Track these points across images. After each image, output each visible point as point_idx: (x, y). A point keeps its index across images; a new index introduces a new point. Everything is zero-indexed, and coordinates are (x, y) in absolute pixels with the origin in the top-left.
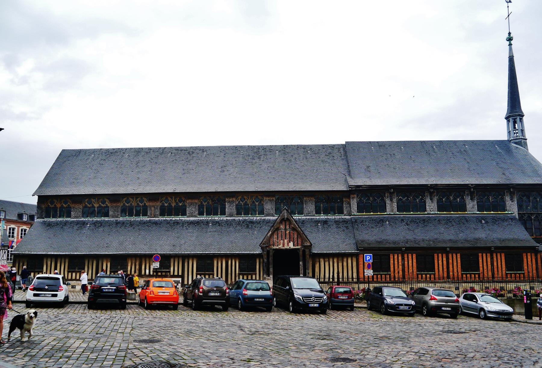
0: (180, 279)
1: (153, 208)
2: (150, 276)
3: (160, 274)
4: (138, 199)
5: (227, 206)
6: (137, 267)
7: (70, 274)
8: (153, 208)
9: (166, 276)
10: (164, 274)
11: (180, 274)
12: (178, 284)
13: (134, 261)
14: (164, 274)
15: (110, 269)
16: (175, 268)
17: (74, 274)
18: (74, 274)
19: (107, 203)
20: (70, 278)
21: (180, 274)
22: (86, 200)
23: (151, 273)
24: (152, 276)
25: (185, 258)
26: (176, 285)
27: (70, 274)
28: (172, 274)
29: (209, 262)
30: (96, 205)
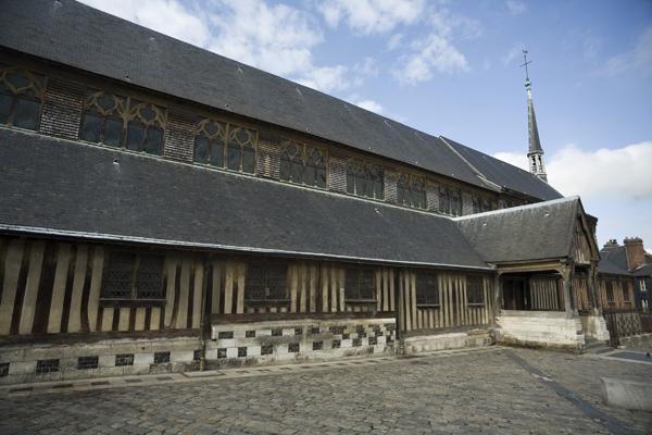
0: (393, 320)
1: (267, 159)
2: (339, 315)
3: (357, 309)
4: (236, 130)
5: (386, 185)
6: (312, 293)
7: (108, 314)
8: (267, 159)
9: (368, 315)
10: (365, 309)
11: (393, 309)
12: (392, 333)
13: (304, 276)
14: (365, 309)
15: (246, 296)
16: (383, 293)
17: (125, 314)
18: (125, 314)
19: (157, 118)
20: (107, 325)
21: (393, 309)
22: (97, 95)
23: (342, 309)
24: (344, 315)
25: (399, 270)
26: (389, 334)
27: (108, 314)
28: (379, 309)
29: (430, 282)
30: (126, 117)
